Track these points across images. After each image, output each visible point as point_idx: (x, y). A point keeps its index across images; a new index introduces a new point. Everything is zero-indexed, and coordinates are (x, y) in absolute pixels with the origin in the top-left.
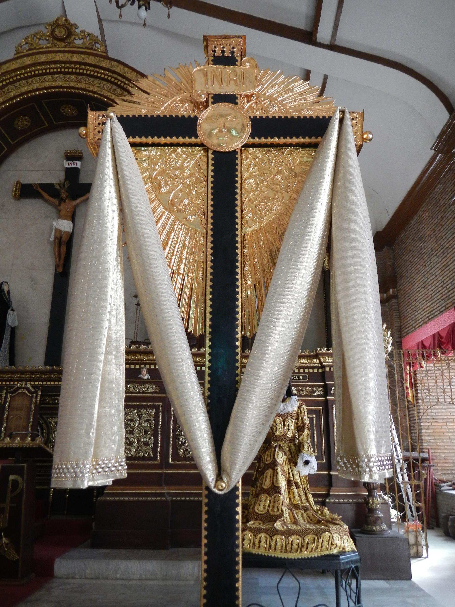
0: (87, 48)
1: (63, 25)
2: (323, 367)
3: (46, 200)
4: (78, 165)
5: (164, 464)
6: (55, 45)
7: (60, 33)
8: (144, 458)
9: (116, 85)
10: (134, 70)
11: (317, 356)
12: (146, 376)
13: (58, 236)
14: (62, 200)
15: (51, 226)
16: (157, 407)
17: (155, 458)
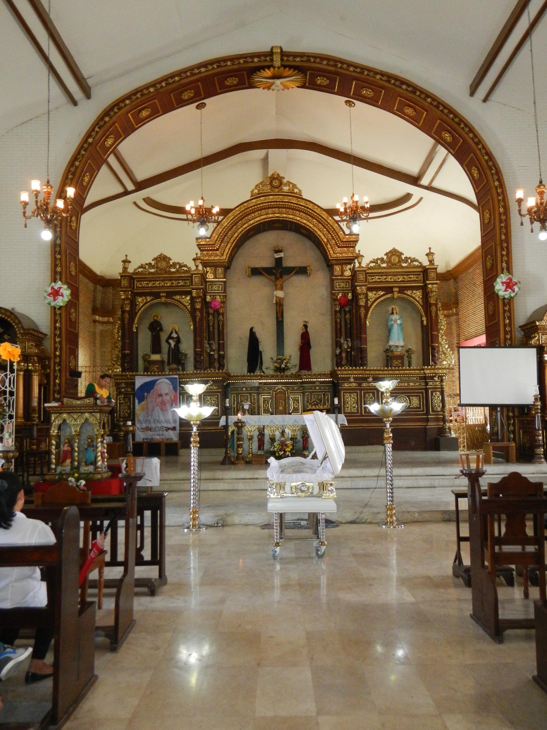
0: (291, 193)
1: (277, 178)
2: (426, 374)
3: (267, 277)
4: (282, 255)
6: (273, 191)
7: (276, 183)
8: (354, 413)
9: (309, 215)
10: (319, 206)
11: (423, 369)
12: (352, 380)
13: (278, 301)
14: (277, 278)
15: (273, 294)
16: (357, 393)
17: (358, 413)
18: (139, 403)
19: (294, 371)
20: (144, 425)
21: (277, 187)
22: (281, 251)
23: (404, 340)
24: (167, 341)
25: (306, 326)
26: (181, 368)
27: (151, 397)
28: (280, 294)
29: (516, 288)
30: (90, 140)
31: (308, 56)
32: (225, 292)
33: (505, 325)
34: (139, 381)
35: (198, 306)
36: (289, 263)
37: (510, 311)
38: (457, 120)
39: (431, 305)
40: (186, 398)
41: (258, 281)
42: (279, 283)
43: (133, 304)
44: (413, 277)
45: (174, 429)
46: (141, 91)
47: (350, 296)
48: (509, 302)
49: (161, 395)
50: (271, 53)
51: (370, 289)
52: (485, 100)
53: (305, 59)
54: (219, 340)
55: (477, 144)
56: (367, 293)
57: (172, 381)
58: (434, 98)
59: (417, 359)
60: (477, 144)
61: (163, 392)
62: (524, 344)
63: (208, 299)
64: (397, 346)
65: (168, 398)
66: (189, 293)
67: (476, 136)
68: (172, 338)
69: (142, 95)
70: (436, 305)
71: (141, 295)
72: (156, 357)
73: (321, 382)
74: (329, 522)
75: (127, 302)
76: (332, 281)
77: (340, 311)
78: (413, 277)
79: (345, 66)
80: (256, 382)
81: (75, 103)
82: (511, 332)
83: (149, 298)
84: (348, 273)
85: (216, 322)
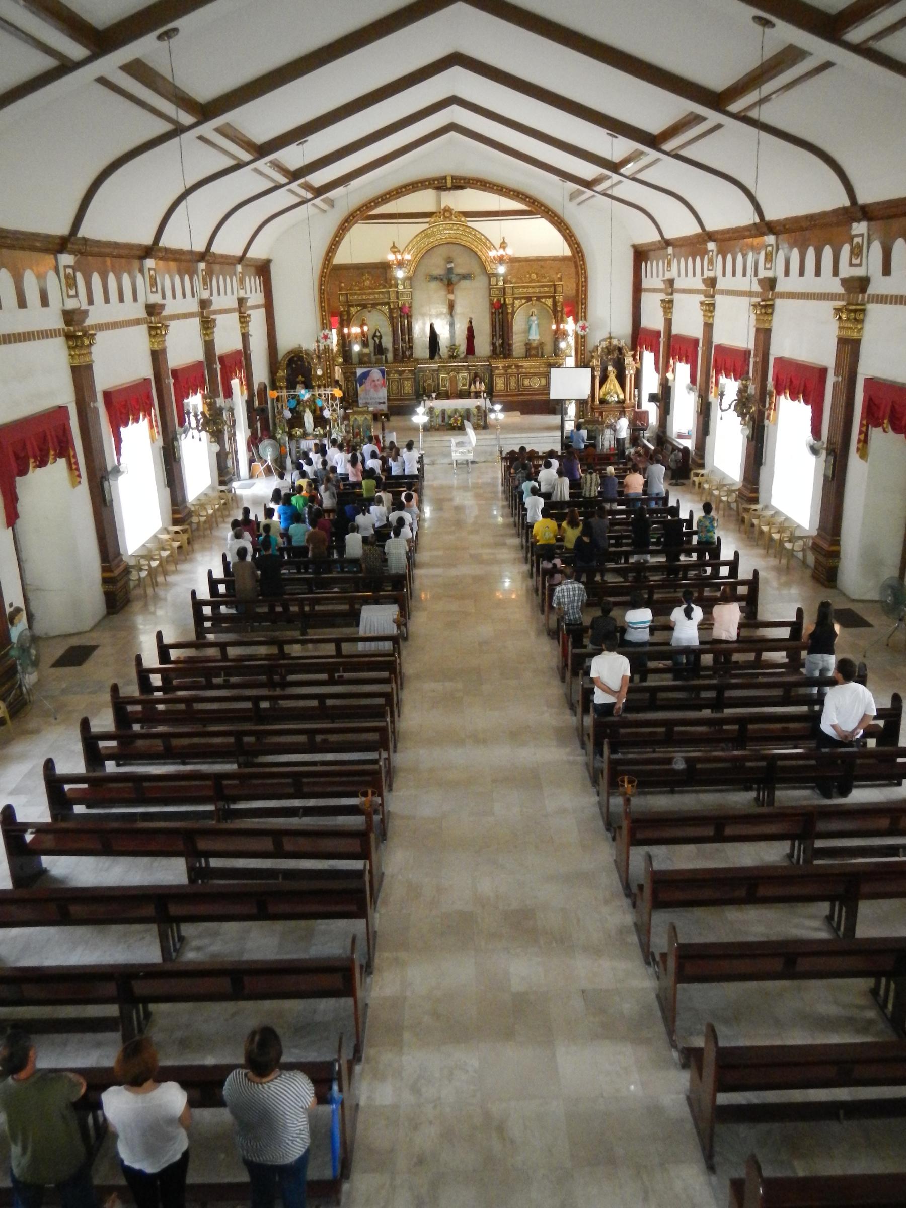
4: (452, 265)
5: (507, 391)
18: (360, 385)
19: (462, 356)
20: (364, 401)
21: (448, 218)
22: (452, 262)
23: (540, 334)
24: (373, 338)
25: (471, 322)
26: (384, 357)
27: (368, 382)
28: (451, 297)
29: (587, 330)
30: (337, 239)
31: (469, 179)
32: (412, 299)
33: (581, 351)
34: (359, 371)
35: (395, 315)
36: (460, 270)
37: (584, 342)
38: (559, 221)
39: (558, 311)
40: (418, 414)
41: (434, 285)
42: (450, 288)
43: (348, 312)
44: (546, 289)
45: (384, 403)
46: (366, 205)
47: (502, 302)
48: (583, 337)
49: (374, 381)
50: (445, 178)
51: (517, 299)
52: (579, 204)
53: (467, 181)
54: (409, 335)
55: (571, 237)
56: (514, 303)
57: (382, 372)
58: (546, 207)
59: (548, 348)
60: (571, 237)
61: (376, 379)
62: (586, 366)
63: (400, 305)
64: (534, 340)
65: (379, 382)
66: (388, 304)
67: (570, 231)
68: (377, 336)
69: (367, 208)
70: (562, 311)
71: (352, 306)
72: (366, 351)
73: (481, 365)
74: (473, 462)
75: (345, 313)
76: (490, 290)
77: (495, 312)
78: (546, 289)
79: (491, 186)
80: (435, 366)
81: (325, 211)
82: (584, 354)
83: (359, 308)
84: (501, 283)
85: (406, 322)
